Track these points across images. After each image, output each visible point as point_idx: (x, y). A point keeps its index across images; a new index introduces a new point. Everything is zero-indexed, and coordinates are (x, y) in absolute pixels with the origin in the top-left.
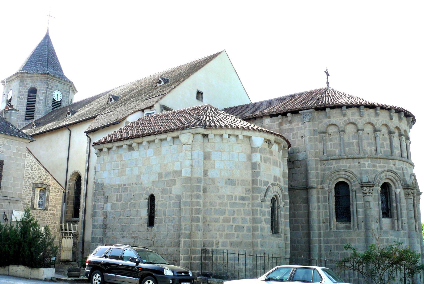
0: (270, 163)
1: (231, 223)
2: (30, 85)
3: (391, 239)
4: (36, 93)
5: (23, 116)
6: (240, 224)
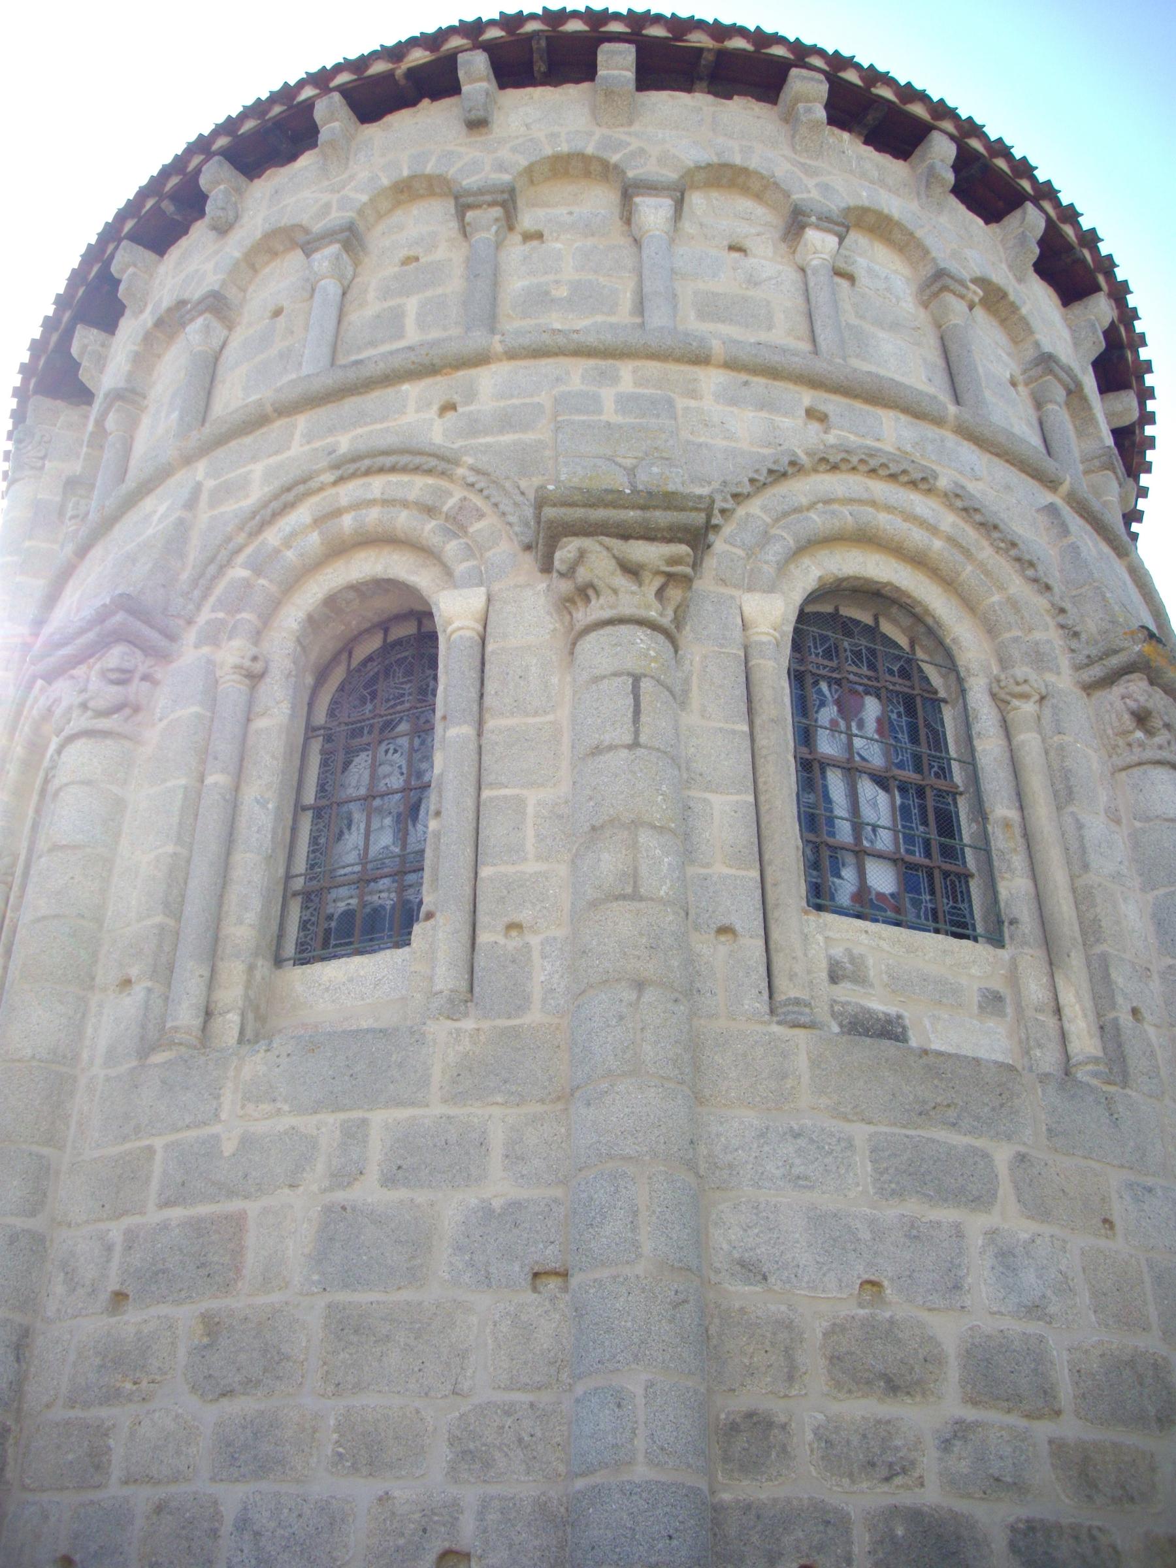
3: (247, 1142)
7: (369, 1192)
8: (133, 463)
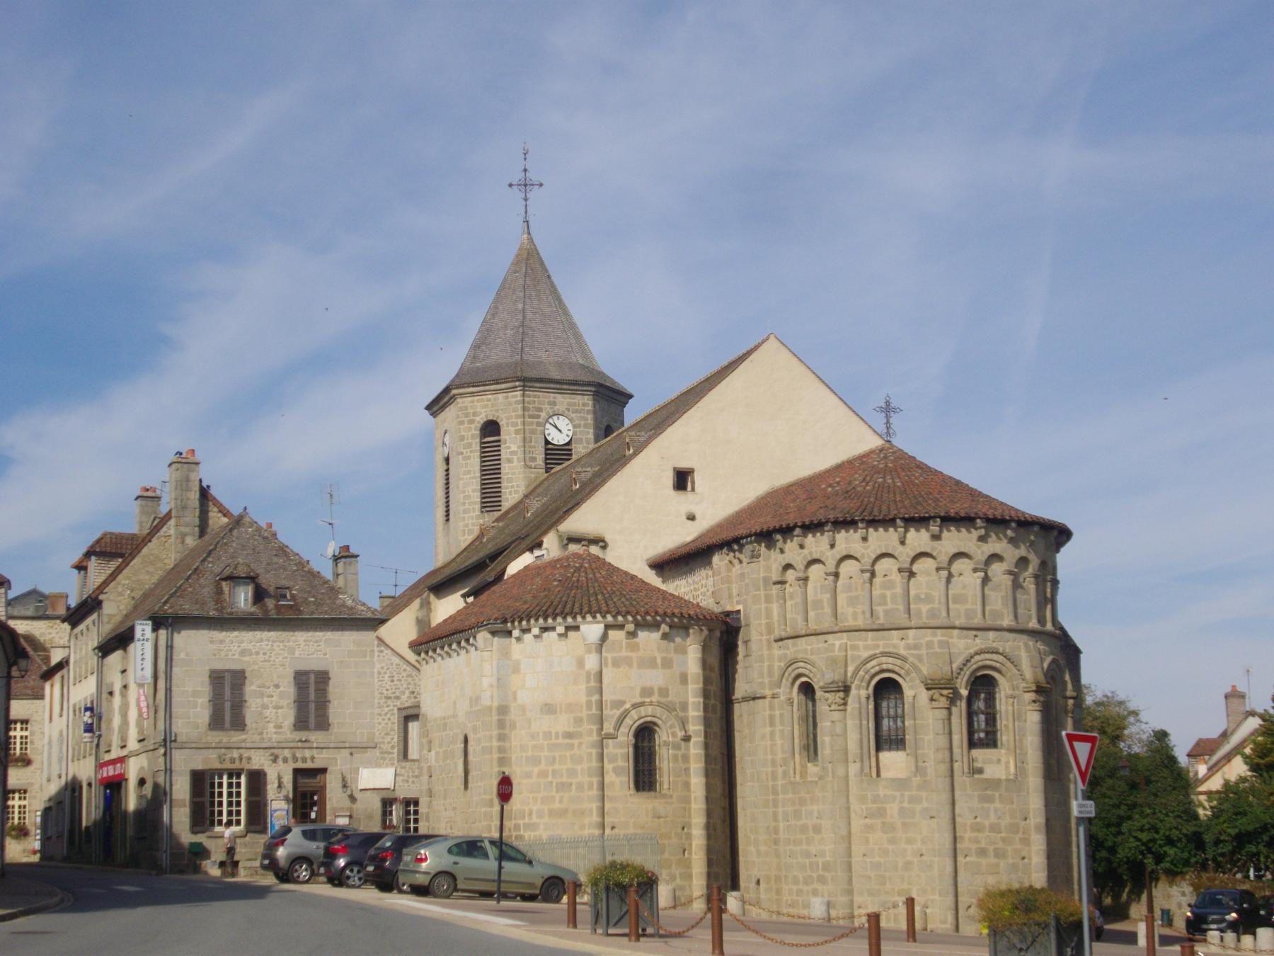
0: (630, 665)
1: (550, 779)
2: (483, 415)
4: (498, 434)
5: (475, 503)
6: (564, 779)
7: (906, 805)
8: (809, 599)
